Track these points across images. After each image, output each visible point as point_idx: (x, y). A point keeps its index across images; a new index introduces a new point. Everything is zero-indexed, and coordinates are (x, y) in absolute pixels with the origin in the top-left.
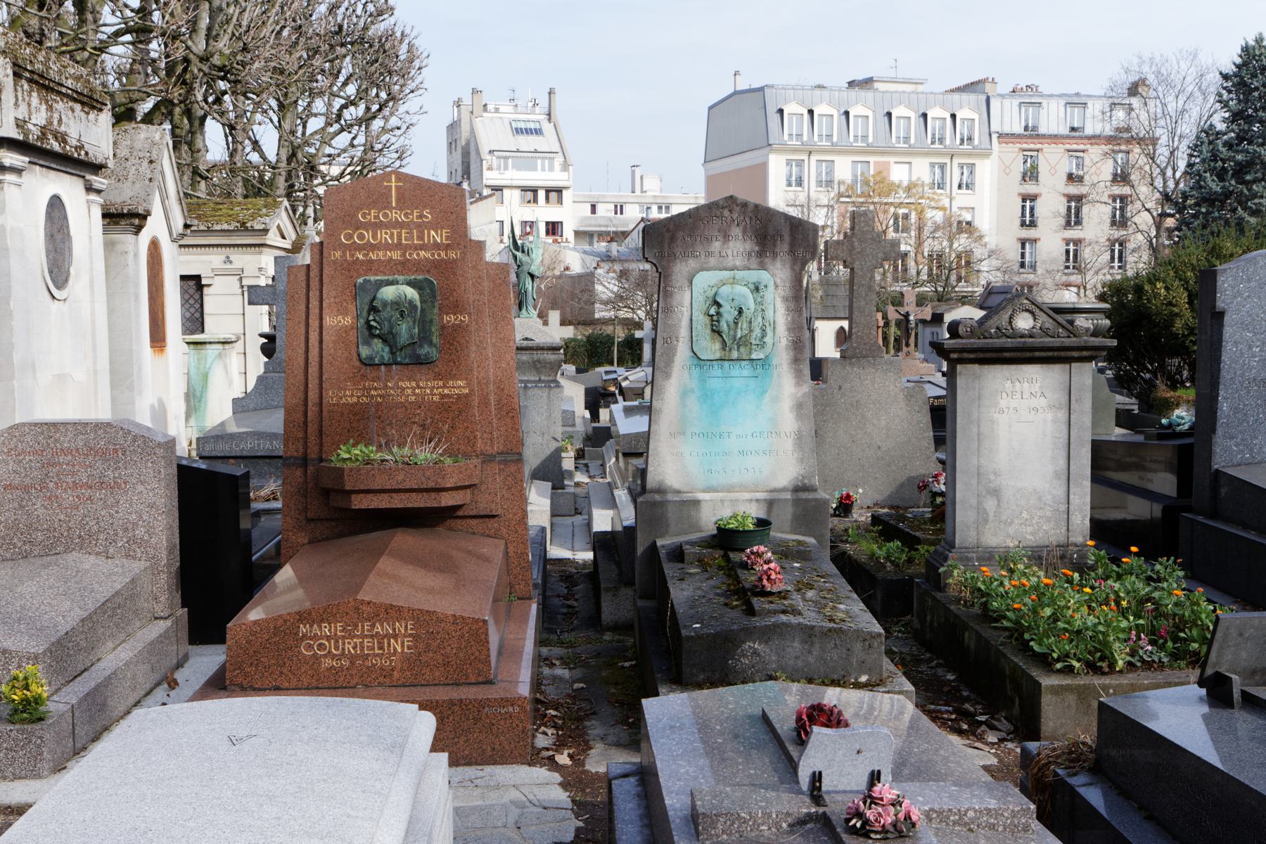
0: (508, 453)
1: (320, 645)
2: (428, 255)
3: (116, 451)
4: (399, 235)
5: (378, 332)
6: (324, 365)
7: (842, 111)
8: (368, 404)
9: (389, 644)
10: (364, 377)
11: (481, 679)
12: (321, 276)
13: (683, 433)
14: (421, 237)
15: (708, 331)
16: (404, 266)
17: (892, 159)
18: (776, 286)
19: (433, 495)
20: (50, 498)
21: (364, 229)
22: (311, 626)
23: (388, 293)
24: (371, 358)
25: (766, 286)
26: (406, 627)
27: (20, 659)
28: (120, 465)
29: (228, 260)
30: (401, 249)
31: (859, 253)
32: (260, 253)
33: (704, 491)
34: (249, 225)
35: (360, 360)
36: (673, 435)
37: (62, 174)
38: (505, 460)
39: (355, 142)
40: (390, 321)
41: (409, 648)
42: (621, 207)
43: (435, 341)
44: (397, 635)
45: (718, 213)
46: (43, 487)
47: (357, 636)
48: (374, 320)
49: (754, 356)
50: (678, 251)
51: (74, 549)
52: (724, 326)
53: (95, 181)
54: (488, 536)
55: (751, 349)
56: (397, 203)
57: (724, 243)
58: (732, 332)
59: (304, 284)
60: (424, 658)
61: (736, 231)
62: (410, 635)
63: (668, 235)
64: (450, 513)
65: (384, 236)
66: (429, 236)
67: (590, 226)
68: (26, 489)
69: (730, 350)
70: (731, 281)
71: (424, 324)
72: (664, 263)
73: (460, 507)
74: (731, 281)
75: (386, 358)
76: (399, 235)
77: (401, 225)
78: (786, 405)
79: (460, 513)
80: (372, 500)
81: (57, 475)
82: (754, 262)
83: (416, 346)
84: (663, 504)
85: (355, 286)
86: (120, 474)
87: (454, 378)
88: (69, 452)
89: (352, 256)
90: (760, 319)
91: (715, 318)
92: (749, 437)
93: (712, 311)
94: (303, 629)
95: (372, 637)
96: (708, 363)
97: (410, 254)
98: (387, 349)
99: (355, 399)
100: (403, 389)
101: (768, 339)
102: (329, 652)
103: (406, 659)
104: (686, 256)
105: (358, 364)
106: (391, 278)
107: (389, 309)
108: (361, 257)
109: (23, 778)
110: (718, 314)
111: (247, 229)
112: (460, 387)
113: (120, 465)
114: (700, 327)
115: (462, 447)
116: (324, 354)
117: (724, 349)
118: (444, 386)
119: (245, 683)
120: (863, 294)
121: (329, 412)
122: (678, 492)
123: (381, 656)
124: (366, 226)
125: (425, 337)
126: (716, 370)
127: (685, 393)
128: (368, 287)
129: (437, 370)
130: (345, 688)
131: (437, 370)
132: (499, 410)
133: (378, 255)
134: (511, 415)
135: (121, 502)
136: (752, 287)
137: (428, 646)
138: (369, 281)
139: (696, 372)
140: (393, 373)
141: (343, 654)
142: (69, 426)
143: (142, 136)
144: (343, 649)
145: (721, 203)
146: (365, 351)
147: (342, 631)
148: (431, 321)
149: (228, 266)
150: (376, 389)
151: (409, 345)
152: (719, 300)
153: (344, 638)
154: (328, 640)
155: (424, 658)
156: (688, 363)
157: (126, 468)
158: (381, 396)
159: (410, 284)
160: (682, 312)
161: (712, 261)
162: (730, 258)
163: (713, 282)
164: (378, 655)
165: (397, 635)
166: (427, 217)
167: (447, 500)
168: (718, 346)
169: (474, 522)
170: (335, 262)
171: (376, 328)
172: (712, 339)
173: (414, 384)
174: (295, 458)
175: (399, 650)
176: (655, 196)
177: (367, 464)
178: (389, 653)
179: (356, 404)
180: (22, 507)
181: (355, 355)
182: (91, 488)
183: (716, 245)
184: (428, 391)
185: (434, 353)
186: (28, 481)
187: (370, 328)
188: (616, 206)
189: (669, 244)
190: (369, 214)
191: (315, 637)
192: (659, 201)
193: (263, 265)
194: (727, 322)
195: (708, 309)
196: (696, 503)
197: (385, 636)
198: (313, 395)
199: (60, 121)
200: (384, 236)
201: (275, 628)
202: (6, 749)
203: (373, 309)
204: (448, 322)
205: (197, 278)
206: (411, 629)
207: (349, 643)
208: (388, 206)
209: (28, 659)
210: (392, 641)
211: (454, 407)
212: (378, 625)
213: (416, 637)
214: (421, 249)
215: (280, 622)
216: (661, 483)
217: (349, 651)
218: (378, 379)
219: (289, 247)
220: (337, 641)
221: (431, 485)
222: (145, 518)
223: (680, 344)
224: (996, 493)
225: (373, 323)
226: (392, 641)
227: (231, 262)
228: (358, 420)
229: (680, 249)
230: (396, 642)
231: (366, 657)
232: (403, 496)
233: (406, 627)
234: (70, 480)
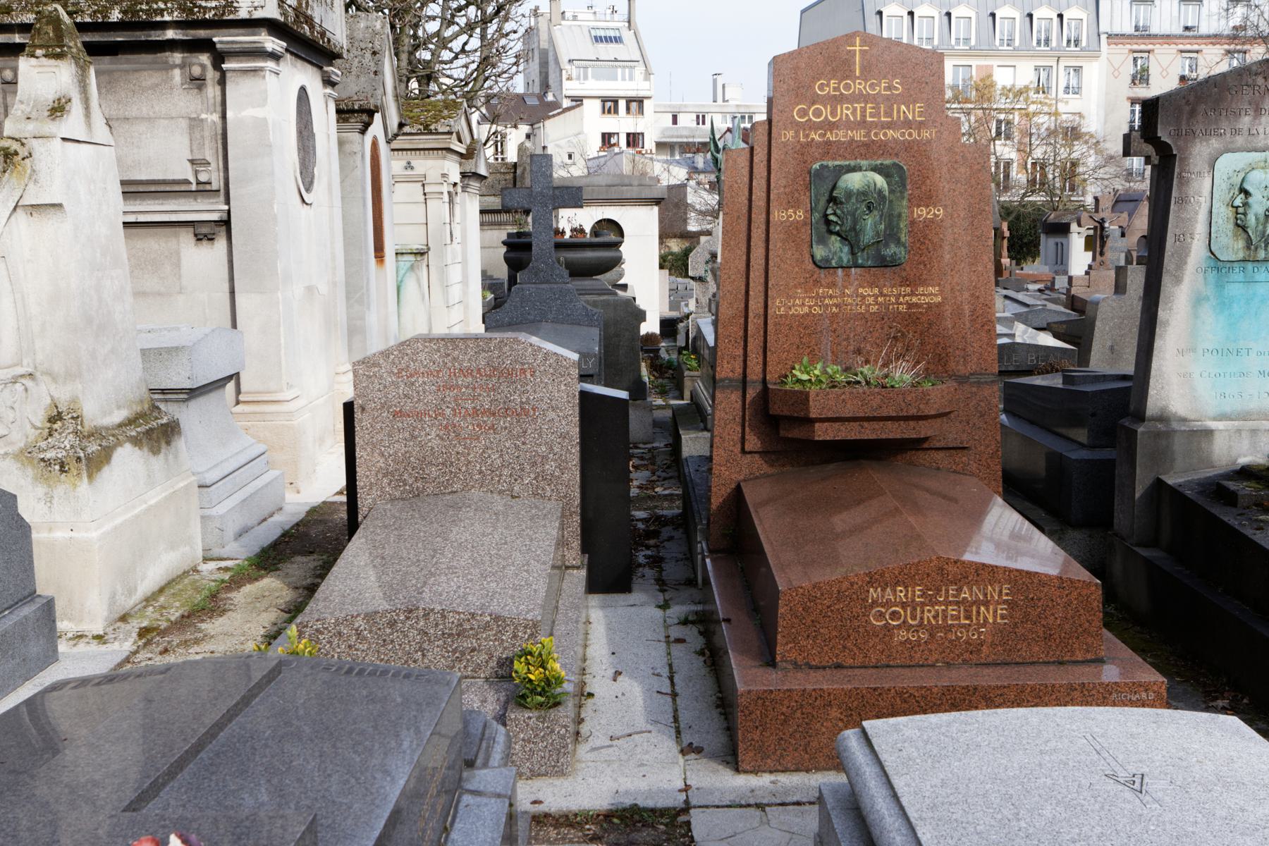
0: (981, 374)
1: (894, 613)
2: (897, 135)
3: (523, 371)
4: (864, 110)
5: (838, 228)
6: (771, 269)
7: (945, 11)
8: (822, 315)
9: (978, 613)
10: (817, 283)
11: (1089, 656)
12: (769, 161)
13: (1193, 350)
14: (889, 113)
15: (1231, 226)
16: (868, 148)
17: (994, 62)
19: (912, 423)
20: (446, 427)
21: (821, 103)
22: (883, 590)
23: (854, 181)
24: (827, 260)
26: (1001, 592)
27: (516, 628)
28: (529, 388)
29: (409, 166)
30: (865, 128)
32: (444, 158)
33: (1215, 419)
34: (432, 127)
35: (814, 263)
36: (1181, 352)
37: (306, 64)
38: (979, 383)
39: (467, 48)
40: (853, 215)
41: (1003, 617)
42: (704, 117)
43: (903, 239)
44: (988, 602)
45: (1250, 81)
46: (439, 413)
47: (940, 603)
48: (835, 214)
50: (1198, 128)
51: (473, 487)
52: (1251, 220)
54: (955, 472)
56: (861, 72)
57: (1255, 118)
58: (1261, 227)
59: (746, 172)
60: (1020, 631)
62: (1005, 602)
63: (1187, 108)
64: (916, 444)
65: (845, 111)
66: (899, 112)
67: (672, 137)
68: (419, 416)
69: (1256, 249)
70: (1262, 164)
71: (892, 221)
72: (1181, 143)
73: (926, 439)
74: (1262, 164)
75: (845, 260)
76: (864, 110)
77: (866, 98)
79: (926, 445)
80: (840, 430)
81: (456, 400)
83: (881, 246)
84: (1169, 434)
85: (810, 173)
86: (528, 398)
87: (924, 283)
88: (469, 371)
89: (807, 136)
91: (1241, 210)
93: (1238, 202)
94: (873, 593)
95: (957, 603)
96: (1228, 265)
97: (876, 134)
98: (846, 249)
99: (806, 310)
100: (864, 297)
102: (904, 622)
103: (998, 630)
104: (1208, 134)
105: (811, 266)
106: (852, 163)
107: (853, 200)
108: (817, 138)
109: (543, 775)
110: (1245, 204)
111: (431, 133)
112: (931, 294)
113: (529, 388)
114: (1220, 221)
115: (932, 367)
116: (771, 256)
117: (1248, 248)
118: (912, 294)
119: (799, 659)
121: (776, 324)
122: (1184, 420)
123: (967, 627)
124: (827, 100)
125: (891, 235)
127: (1198, 301)
128: (826, 174)
130: (922, 666)
131: (904, 274)
132: (973, 321)
133: (837, 135)
134: (986, 327)
135: (529, 431)
137: (1027, 615)
138: (827, 166)
139: (1212, 276)
140: (852, 278)
141: (921, 624)
142: (469, 342)
143: (362, 25)
144: (922, 618)
145: (1254, 68)
146: (820, 252)
147: (921, 596)
148: (899, 215)
149: (409, 172)
150: (831, 297)
151: (873, 244)
152: (1247, 186)
153: (923, 605)
154: (903, 608)
155: (1020, 631)
156: (1204, 266)
157: (535, 392)
158: (837, 306)
159: (875, 169)
160: (1198, 202)
161: (1240, 140)
162: (1262, 136)
163: (1240, 166)
164: (964, 626)
165: (988, 602)
166: (897, 89)
167: (924, 430)
168: (1241, 244)
169: (941, 454)
170: (785, 144)
171: (836, 223)
172: (1235, 235)
173: (876, 291)
174: (731, 380)
175: (991, 621)
176: (737, 106)
177: (834, 387)
178: (978, 624)
179: (807, 315)
180: (413, 437)
181: (807, 256)
182: (494, 414)
183: (1246, 121)
184: (893, 300)
185: (901, 252)
186: (421, 407)
187: (828, 222)
188: (698, 117)
189: (1188, 120)
190: (828, 85)
191: (888, 604)
192: (742, 110)
193: (446, 172)
194: (1256, 215)
195: (1233, 199)
196: (1209, 433)
197: (975, 602)
198: (756, 305)
200: (845, 111)
201: (839, 592)
202: (523, 740)
203: (832, 200)
204: (920, 216)
206: (1007, 594)
207: (929, 611)
208: (849, 74)
209: (525, 627)
210: (982, 608)
211: (924, 319)
212: (965, 588)
213: (1012, 605)
214: (889, 128)
215: (845, 585)
216: (1164, 409)
217: (929, 621)
218: (833, 285)
219: (464, 151)
220: (914, 609)
221: (913, 411)
222: (556, 450)
223: (1195, 242)
225: (832, 218)
226: (982, 608)
227: (412, 168)
228: (810, 334)
229: (1201, 126)
230: (988, 610)
231: (948, 628)
232: (875, 425)
233: (1001, 592)
234: (469, 405)
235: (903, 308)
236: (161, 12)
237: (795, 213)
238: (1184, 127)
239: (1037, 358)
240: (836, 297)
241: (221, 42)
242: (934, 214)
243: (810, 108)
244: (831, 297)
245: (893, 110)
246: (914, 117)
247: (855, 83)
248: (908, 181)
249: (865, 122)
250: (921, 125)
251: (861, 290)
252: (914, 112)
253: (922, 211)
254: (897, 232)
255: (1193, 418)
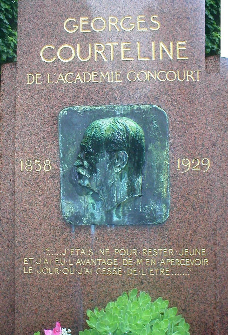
43: (165, 195)
66: (157, 51)
100: (120, 258)
108: (65, 81)
118: (176, 256)
128: (75, 120)
129: (166, 234)
138: (76, 111)
148: (160, 167)
150: (83, 258)
159: (131, 115)
166: (155, 26)
170: (31, 88)
173: (134, 252)
190: (77, 23)
204: (183, 168)
237: (43, 164)
240: (89, 258)
242: (200, 165)
243: (57, 49)
244: (83, 258)
245: (150, 50)
246: (175, 56)
247: (106, 20)
248: (169, 128)
249: (119, 62)
251: (116, 251)
252: (174, 52)
253: (186, 162)
254: (157, 186)
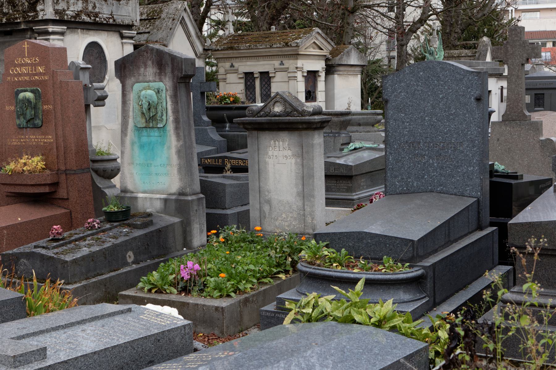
13: (133, 163)
14: (35, 70)
15: (140, 113)
18: (167, 90)
25: (162, 90)
29: (282, 64)
31: (511, 54)
32: (297, 59)
34: (289, 44)
49: (159, 126)
53: (125, 33)
55: (157, 122)
61: (150, 63)
65: (24, 70)
70: (148, 88)
74: (148, 88)
78: (173, 151)
82: (157, 78)
87: (48, 134)
90: (160, 107)
92: (159, 166)
99: (16, 143)
100: (31, 139)
101: (164, 117)
108: (16, 79)
114: (137, 111)
117: (146, 122)
118: (44, 139)
120: (514, 80)
122: (133, 192)
126: (145, 133)
127: (133, 144)
136: (156, 91)
139: (136, 133)
148: (39, 108)
150: (23, 139)
166: (37, 61)
168: (144, 120)
172: (142, 117)
183: (142, 69)
184: (39, 140)
189: (124, 72)
190: (19, 60)
196: (136, 198)
199: (94, 7)
200: (24, 70)
205: (267, 73)
214: (36, 76)
218: (23, 134)
224: (269, 202)
235: (42, 144)
236: (16, 18)
238: (123, 73)
239: (335, 169)
241: (36, 29)
250: (44, 74)
251: (30, 136)
255: (135, 191)
